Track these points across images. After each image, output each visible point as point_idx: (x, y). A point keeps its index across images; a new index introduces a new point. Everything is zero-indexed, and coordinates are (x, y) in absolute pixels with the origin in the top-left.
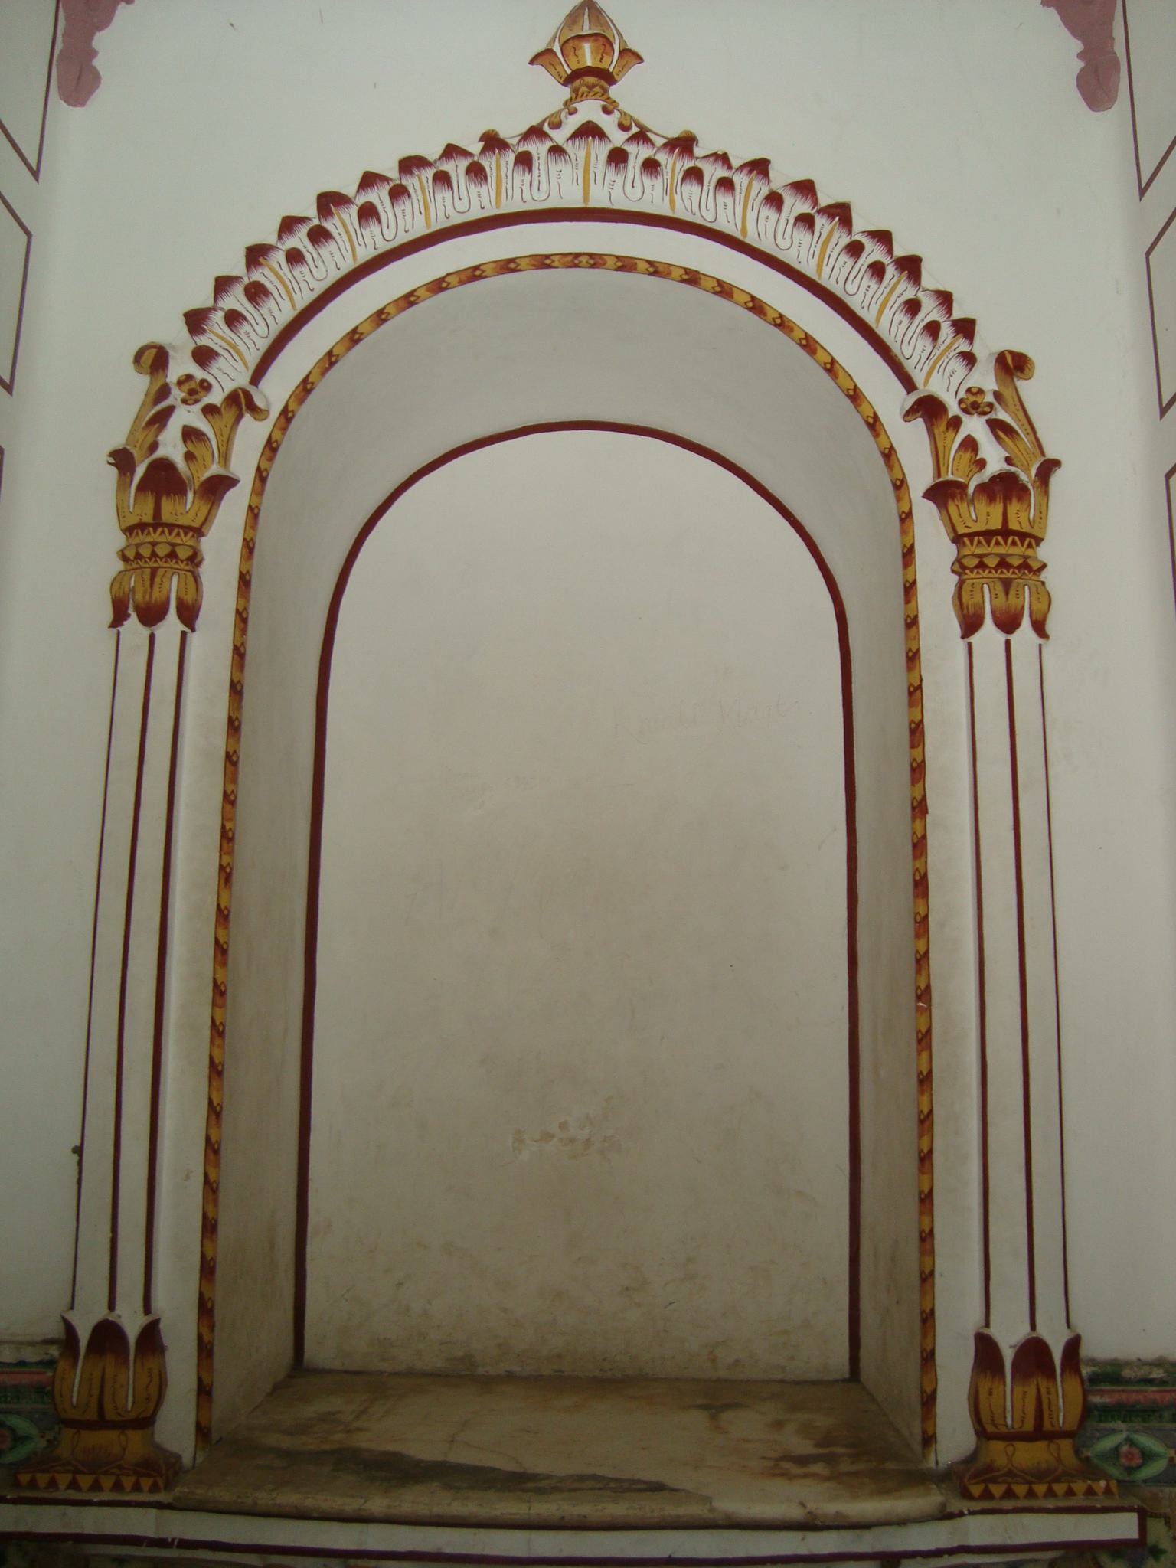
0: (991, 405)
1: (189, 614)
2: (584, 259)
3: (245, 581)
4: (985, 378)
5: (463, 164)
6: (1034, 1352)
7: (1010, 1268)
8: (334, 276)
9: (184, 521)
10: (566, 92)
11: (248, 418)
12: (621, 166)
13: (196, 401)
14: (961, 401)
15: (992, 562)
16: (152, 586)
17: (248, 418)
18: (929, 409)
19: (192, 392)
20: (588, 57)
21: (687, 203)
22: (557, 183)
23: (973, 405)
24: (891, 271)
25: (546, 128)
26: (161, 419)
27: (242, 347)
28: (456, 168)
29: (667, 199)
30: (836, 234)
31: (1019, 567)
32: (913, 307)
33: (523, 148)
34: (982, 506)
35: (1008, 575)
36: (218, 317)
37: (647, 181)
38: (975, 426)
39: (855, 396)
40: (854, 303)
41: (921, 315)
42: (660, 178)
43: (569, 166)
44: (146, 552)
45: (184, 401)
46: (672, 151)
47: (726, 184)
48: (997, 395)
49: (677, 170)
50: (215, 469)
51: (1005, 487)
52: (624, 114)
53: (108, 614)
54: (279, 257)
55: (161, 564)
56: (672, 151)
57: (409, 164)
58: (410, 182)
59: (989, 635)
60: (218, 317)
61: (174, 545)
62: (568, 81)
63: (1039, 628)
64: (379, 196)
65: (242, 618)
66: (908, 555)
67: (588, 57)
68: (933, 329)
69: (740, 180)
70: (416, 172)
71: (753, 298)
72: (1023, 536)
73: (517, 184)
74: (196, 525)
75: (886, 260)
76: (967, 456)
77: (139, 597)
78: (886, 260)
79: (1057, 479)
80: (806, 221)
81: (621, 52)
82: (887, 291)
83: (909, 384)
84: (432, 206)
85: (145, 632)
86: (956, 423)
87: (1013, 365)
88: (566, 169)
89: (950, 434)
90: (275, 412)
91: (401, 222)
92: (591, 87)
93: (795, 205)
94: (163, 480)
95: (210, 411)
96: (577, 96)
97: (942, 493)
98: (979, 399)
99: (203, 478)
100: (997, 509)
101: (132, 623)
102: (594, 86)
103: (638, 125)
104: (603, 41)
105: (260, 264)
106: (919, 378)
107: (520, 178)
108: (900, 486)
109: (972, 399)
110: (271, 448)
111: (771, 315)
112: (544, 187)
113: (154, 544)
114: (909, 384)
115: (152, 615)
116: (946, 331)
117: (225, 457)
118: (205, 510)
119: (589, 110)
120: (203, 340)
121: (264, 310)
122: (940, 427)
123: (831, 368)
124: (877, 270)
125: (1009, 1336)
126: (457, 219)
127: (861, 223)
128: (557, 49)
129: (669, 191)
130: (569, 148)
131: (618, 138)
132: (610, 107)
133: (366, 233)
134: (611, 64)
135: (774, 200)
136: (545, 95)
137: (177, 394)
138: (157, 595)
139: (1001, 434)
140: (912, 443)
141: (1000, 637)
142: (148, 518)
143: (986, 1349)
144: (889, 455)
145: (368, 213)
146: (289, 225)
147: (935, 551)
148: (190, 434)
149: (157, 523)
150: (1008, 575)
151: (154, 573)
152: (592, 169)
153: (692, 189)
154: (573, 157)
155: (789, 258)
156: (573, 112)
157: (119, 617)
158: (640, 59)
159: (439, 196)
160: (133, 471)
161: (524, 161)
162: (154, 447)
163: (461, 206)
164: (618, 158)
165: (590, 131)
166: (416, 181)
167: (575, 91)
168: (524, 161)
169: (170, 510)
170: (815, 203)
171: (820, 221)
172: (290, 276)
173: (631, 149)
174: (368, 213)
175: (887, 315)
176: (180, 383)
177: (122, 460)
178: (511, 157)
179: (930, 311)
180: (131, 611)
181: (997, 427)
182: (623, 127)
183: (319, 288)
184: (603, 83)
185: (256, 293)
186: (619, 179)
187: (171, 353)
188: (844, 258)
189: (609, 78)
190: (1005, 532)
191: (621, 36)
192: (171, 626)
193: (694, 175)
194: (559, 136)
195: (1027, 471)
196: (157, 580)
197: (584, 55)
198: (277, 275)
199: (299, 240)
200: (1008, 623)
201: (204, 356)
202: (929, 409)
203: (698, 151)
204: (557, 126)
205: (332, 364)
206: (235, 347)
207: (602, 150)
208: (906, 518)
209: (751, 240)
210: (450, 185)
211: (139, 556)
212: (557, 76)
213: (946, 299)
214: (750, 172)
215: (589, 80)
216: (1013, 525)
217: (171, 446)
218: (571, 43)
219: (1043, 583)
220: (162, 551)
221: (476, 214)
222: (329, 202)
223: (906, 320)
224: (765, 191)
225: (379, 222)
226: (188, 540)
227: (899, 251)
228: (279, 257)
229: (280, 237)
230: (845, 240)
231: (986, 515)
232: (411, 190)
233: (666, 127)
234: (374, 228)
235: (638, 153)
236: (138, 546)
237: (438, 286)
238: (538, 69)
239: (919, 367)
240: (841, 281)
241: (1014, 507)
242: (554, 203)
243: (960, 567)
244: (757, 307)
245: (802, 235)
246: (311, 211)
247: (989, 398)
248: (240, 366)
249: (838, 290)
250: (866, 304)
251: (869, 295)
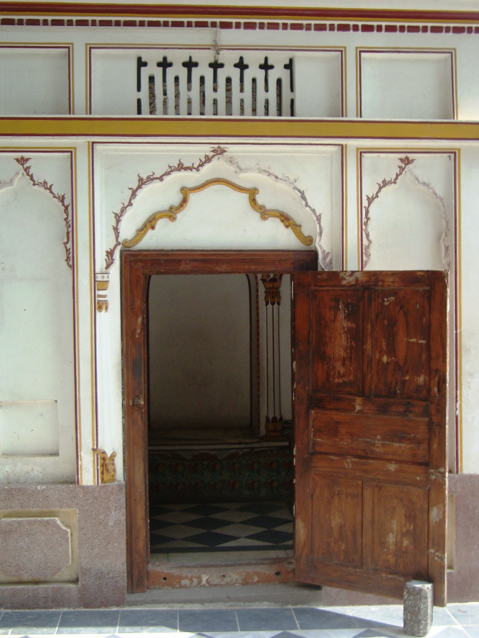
6: (274, 419)
7: (271, 406)
59: (270, 305)
63: (279, 304)
72: (276, 288)
97: (264, 280)
125: (271, 416)
141: (271, 306)
143: (267, 418)
147: (262, 289)
190: (273, 288)
200: (273, 304)
231: (270, 285)
241: (275, 283)
243: (265, 292)
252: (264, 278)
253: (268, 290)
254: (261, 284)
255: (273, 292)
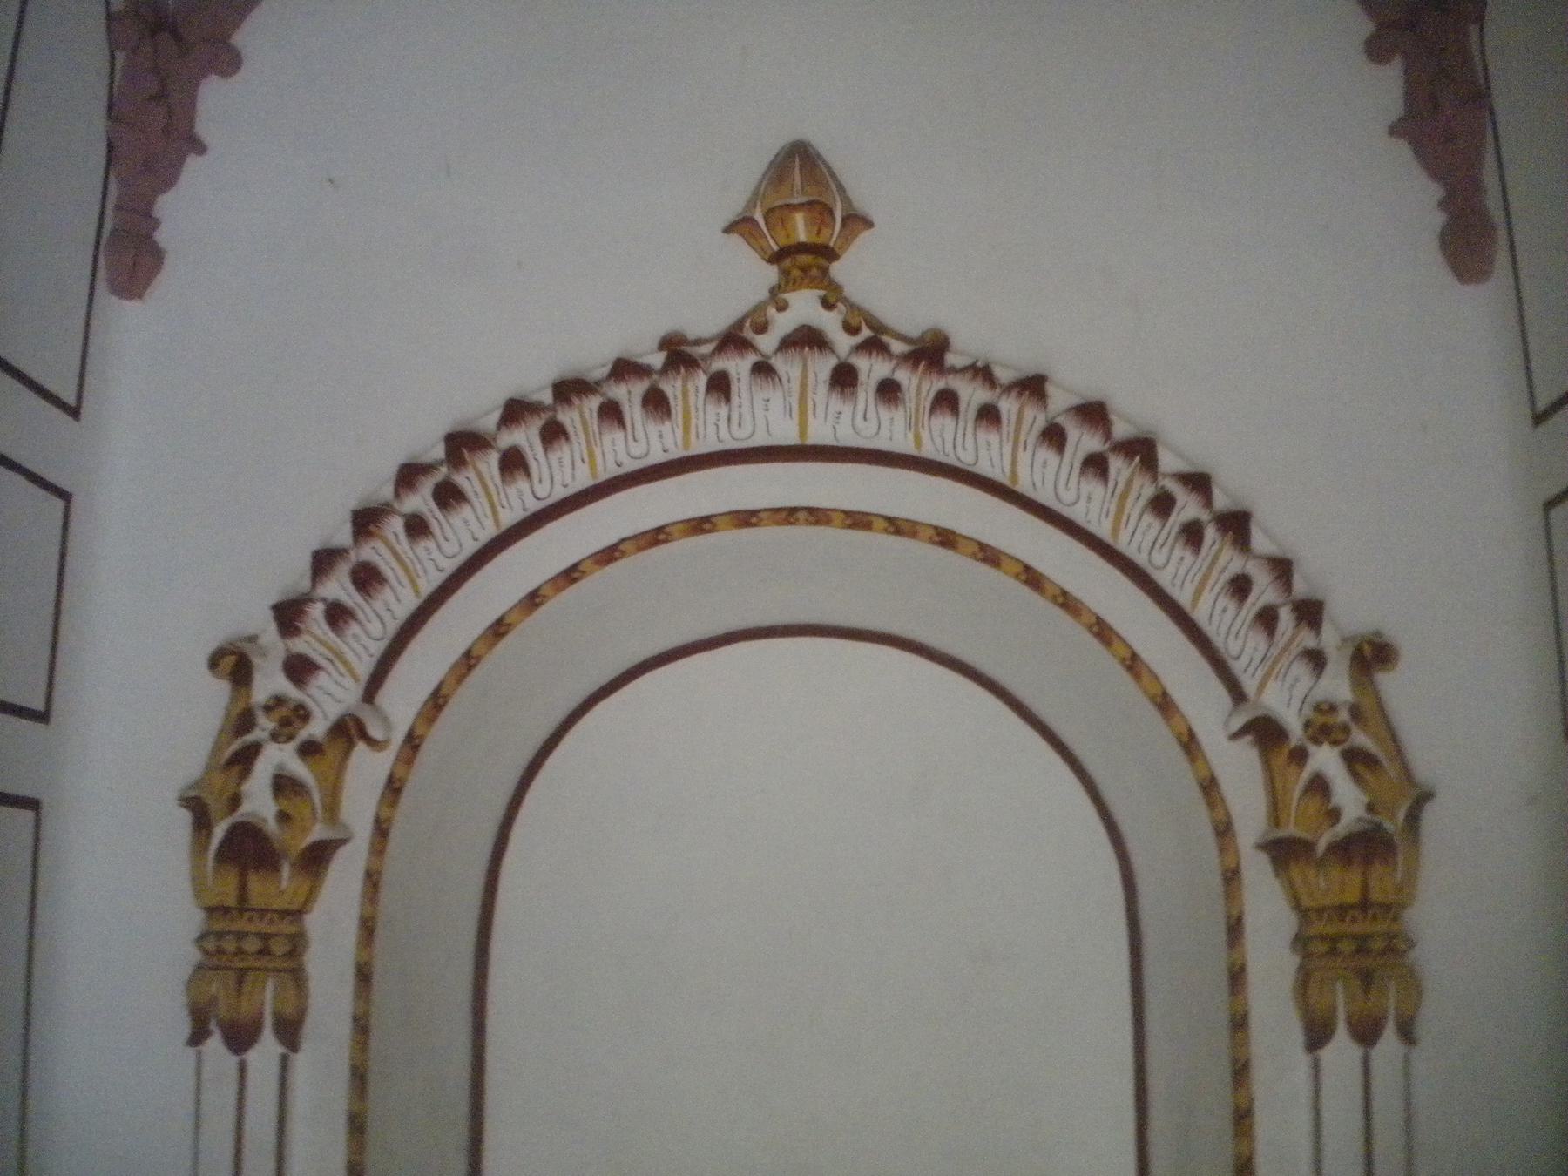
0: (1345, 729)
1: (290, 1032)
2: (801, 516)
3: (364, 976)
4: (1337, 685)
5: (639, 388)
8: (470, 548)
9: (278, 904)
10: (771, 274)
11: (361, 747)
12: (848, 390)
13: (290, 738)
14: (1307, 725)
15: (1346, 947)
16: (239, 992)
17: (361, 747)
18: (1265, 732)
19: (285, 722)
20: (802, 215)
21: (938, 441)
22: (763, 415)
23: (1322, 731)
24: (1210, 533)
25: (748, 333)
26: (244, 759)
27: (350, 656)
28: (629, 394)
29: (911, 436)
30: (1137, 483)
31: (1383, 953)
32: (1240, 587)
33: (718, 364)
34: (1335, 873)
35: (1367, 962)
36: (317, 611)
37: (885, 413)
38: (1325, 759)
39: (1165, 704)
40: (1163, 579)
41: (1251, 598)
42: (901, 408)
43: (779, 394)
44: (230, 945)
45: (275, 737)
46: (915, 366)
47: (988, 415)
48: (1356, 712)
49: (924, 393)
50: (318, 833)
51: (1367, 846)
52: (853, 307)
53: (185, 1027)
54: (395, 525)
55: (251, 962)
56: (915, 366)
57: (569, 389)
58: (568, 417)
59: (1341, 1050)
60: (317, 611)
61: (265, 937)
62: (776, 258)
63: (1407, 1033)
64: (525, 437)
65: (362, 1027)
66: (1235, 929)
67: (802, 215)
68: (1267, 619)
69: (1008, 406)
70: (576, 401)
71: (1027, 568)
73: (711, 418)
74: (294, 907)
75: (1205, 516)
76: (1314, 804)
77: (223, 1011)
78: (1205, 516)
79: (1431, 817)
80: (1096, 465)
81: (845, 220)
82: (1206, 564)
83: (1238, 694)
84: (598, 452)
85: (233, 1060)
86: (1299, 756)
87: (1373, 656)
88: (776, 397)
89: (1293, 769)
90: (398, 737)
91: (558, 472)
92: (805, 270)
93: (1084, 441)
94: (247, 850)
95: (309, 750)
96: (788, 282)
98: (1330, 720)
99: (303, 845)
100: (1354, 878)
101: (215, 1044)
102: (810, 267)
103: (871, 327)
104: (820, 211)
105: (370, 535)
106: (1249, 685)
107: (715, 412)
108: (1224, 831)
109: (1320, 720)
110: (393, 788)
111: (1050, 590)
112: (747, 417)
113: (241, 936)
114: (1238, 694)
115: (240, 1038)
116: (1286, 617)
117: (332, 809)
118: (305, 887)
119: (804, 307)
120: (300, 645)
121: (378, 605)
122: (1280, 759)
123: (1133, 664)
124: (1192, 534)
126: (631, 466)
127: (1168, 461)
128: (759, 216)
129: (913, 425)
130: (778, 363)
131: (844, 343)
132: (832, 300)
133: (511, 491)
134: (832, 237)
135: (1054, 436)
136: (745, 277)
137: (265, 725)
138: (246, 1008)
139: (1360, 768)
140: (1239, 769)
142: (231, 901)
144: (1210, 787)
145: (513, 463)
146: (409, 475)
148: (283, 785)
149: (242, 905)
150: (1367, 962)
151: (240, 982)
152: (810, 395)
153: (944, 422)
154: (784, 379)
155: (1077, 514)
156: (782, 307)
157: (198, 1037)
158: (868, 223)
159: (607, 439)
160: (209, 835)
161: (720, 386)
162: (235, 801)
163: (637, 450)
164: (844, 378)
165: (808, 339)
166: (575, 415)
167: (785, 273)
168: (720, 386)
169: (256, 884)
170: (1108, 435)
171: (1116, 464)
172: (410, 554)
173: (862, 363)
174: (513, 463)
175: (1207, 598)
176: (268, 709)
177: (200, 813)
178: (701, 380)
179: (1264, 591)
180: (213, 1026)
181: (1356, 760)
182: (851, 329)
183: (450, 566)
184: (822, 261)
185: (367, 578)
186: (847, 409)
187: (256, 661)
188: (1148, 518)
189: (830, 254)
191: (846, 200)
192: (268, 1048)
193: (947, 401)
194: (767, 343)
195: (1392, 817)
196: (246, 988)
197: (795, 229)
198: (395, 553)
199: (420, 501)
200: (1366, 1034)
201: (299, 669)
202: (1265, 732)
203: (951, 359)
204: (762, 328)
205: (470, 668)
206: (339, 655)
207: (822, 367)
208: (1232, 877)
209: (1023, 486)
210: (621, 422)
211: (220, 951)
212: (761, 251)
213: (1282, 568)
214: (1020, 394)
215: (805, 262)
216: (1376, 896)
217: (259, 802)
218: (779, 215)
219: (1411, 971)
220: (252, 945)
221: (657, 457)
222: (463, 444)
223: (1232, 606)
224: (1041, 423)
225: (528, 475)
226: (287, 928)
227: (1221, 502)
228: (395, 525)
229: (397, 495)
230: (1149, 491)
232: (570, 430)
233: (908, 315)
234: (522, 484)
235: (872, 369)
236: (220, 935)
237: (609, 555)
238: (735, 239)
239: (1251, 670)
240: (1146, 546)
241: (1377, 870)
242: (760, 440)
243: (1301, 942)
244: (1033, 579)
245: (1092, 487)
246: (439, 452)
247: (1343, 716)
248: (348, 682)
249: (1141, 559)
250: (1178, 582)
251: (1182, 573)
252: (1291, 830)
253: (1321, 927)
254: (1258, 872)
255: (1362, 945)
